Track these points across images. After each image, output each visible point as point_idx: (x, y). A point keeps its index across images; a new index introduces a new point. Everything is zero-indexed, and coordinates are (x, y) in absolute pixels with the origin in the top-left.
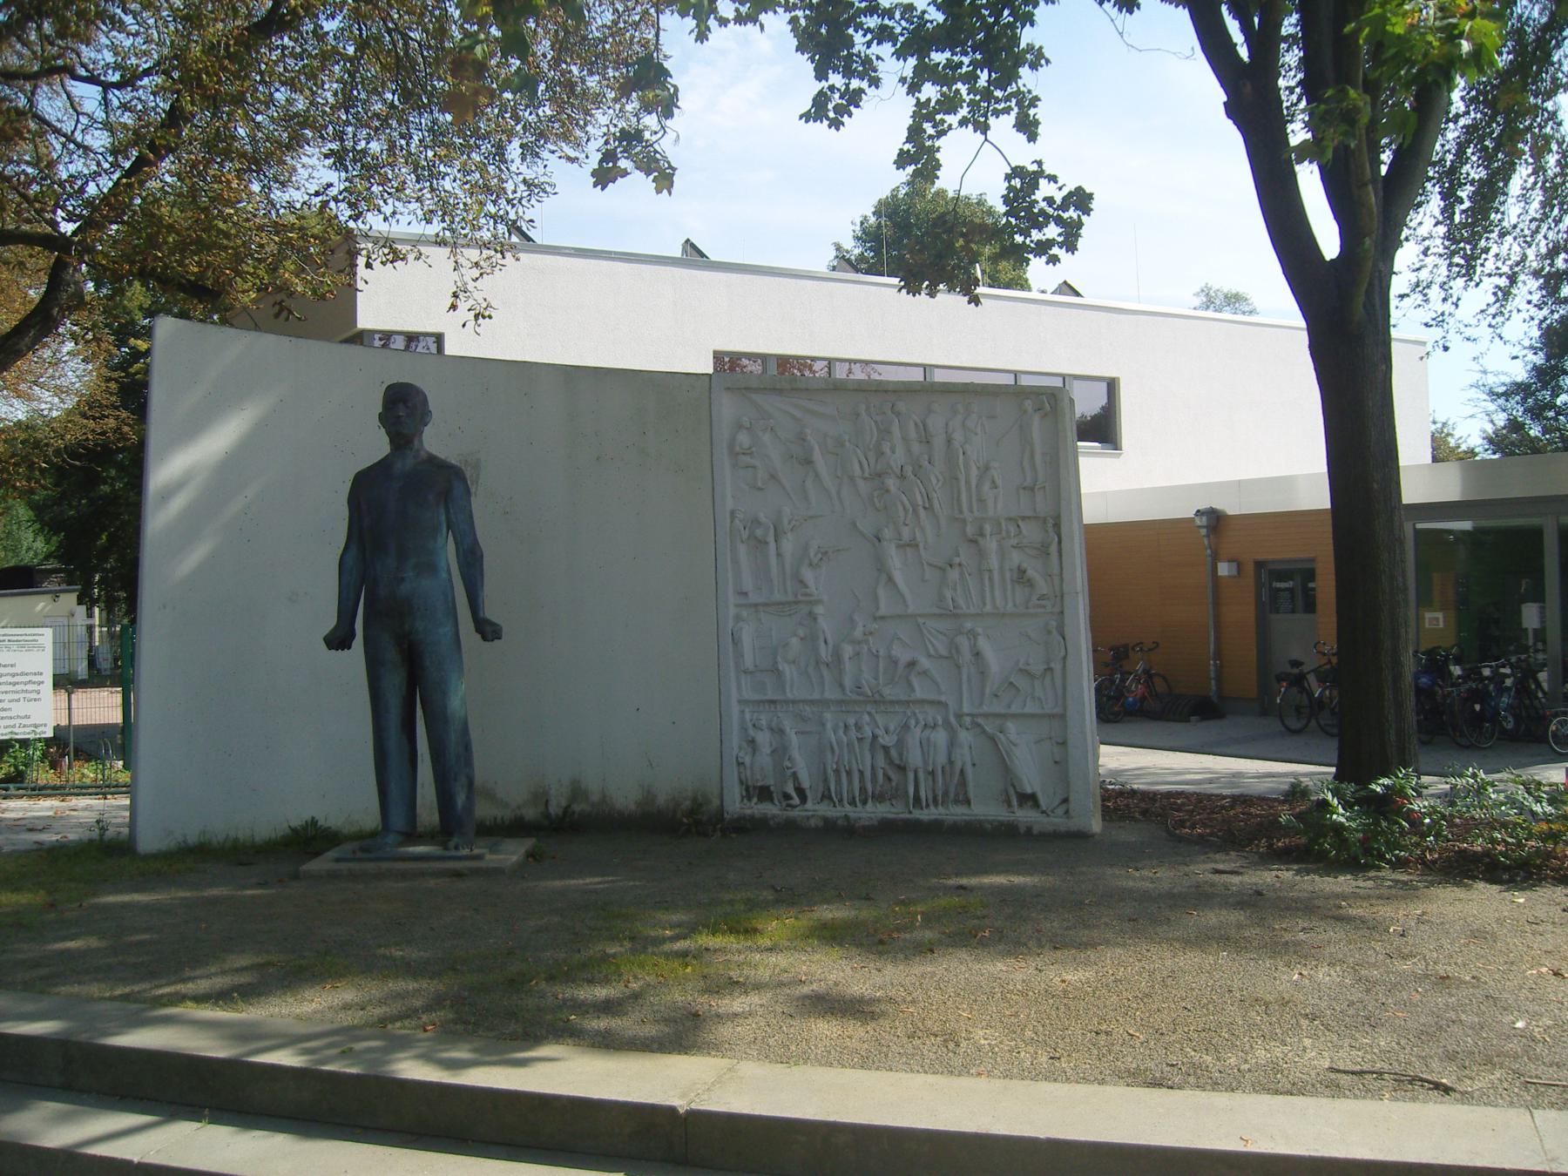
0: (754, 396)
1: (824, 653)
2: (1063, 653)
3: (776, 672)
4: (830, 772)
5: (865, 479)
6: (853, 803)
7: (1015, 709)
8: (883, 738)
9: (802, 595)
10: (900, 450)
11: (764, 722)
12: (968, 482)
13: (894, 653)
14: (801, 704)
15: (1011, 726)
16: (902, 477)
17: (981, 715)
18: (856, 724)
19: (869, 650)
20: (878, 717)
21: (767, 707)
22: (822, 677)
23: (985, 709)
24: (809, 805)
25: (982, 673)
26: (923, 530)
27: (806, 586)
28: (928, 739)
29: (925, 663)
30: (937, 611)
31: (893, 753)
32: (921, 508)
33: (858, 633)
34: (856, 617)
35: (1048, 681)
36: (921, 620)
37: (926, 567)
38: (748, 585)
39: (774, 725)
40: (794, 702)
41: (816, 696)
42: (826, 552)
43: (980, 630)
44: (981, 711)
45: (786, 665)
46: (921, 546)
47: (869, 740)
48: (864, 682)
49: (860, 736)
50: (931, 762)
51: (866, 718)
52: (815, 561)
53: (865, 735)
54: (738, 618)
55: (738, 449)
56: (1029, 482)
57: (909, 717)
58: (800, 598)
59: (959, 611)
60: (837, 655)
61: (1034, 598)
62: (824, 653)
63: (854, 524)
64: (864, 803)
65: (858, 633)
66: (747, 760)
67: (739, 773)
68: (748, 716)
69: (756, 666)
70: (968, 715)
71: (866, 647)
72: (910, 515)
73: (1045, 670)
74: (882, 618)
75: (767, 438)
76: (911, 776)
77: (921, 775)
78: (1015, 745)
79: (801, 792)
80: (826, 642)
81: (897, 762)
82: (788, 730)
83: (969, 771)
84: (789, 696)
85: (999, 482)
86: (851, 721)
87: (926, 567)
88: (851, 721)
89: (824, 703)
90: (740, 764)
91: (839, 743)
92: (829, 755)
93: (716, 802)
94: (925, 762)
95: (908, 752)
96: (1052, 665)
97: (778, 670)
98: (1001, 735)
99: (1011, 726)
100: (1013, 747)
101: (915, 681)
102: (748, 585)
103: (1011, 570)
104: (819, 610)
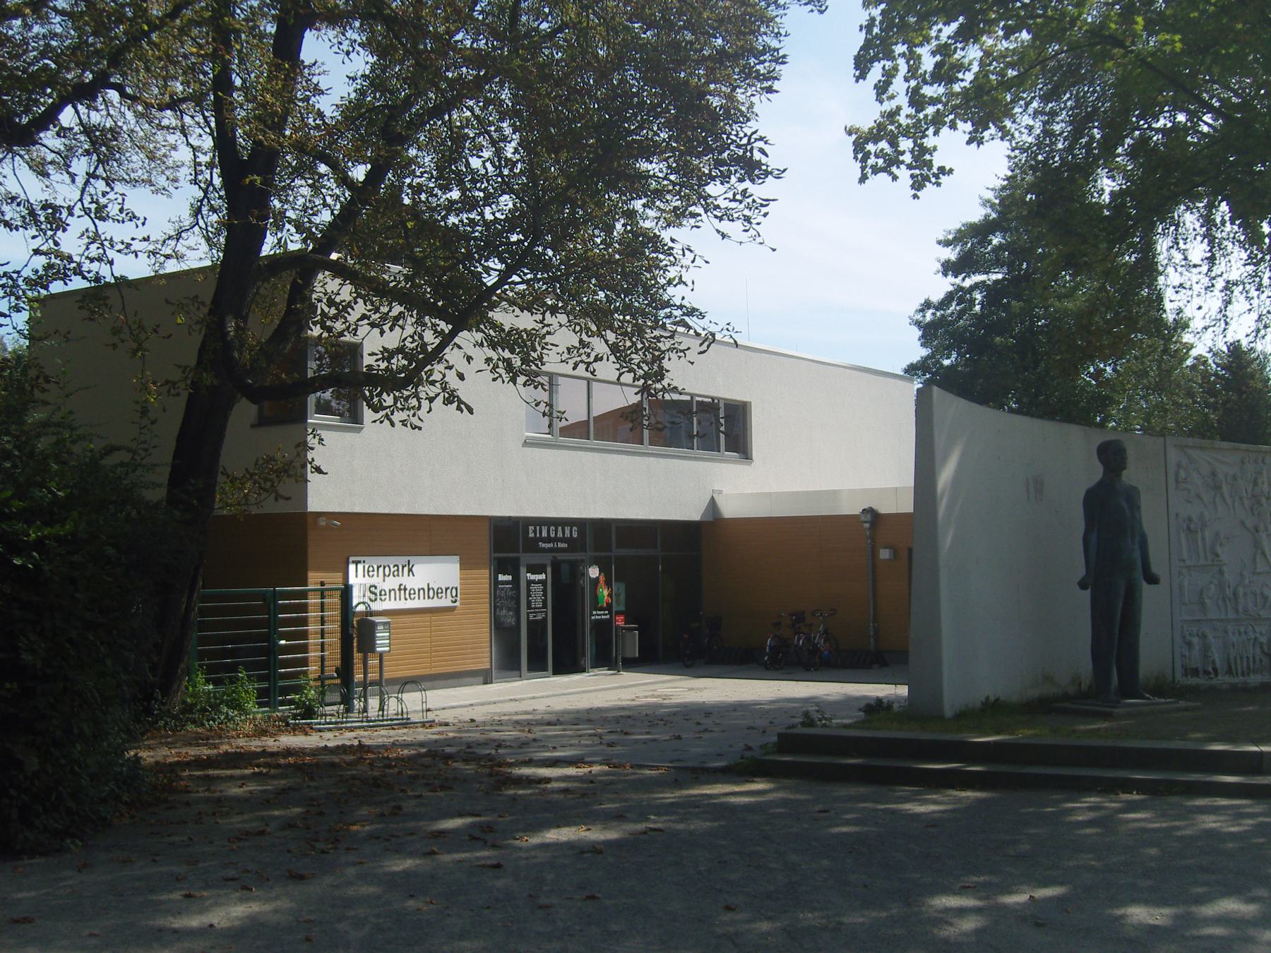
0: (1190, 451)
1: (1228, 592)
3: (1202, 603)
4: (1232, 657)
6: (1243, 675)
22: (1227, 606)
24: (1219, 677)
27: (1217, 556)
38: (1185, 555)
40: (1211, 620)
54: (1180, 573)
60: (1235, 594)
62: (1228, 592)
64: (1249, 674)
65: (1247, 581)
74: (1259, 573)
79: (1215, 670)
86: (1242, 630)
88: (1242, 630)
90: (1183, 656)
93: (1170, 679)
102: (1185, 555)
104: (1225, 569)
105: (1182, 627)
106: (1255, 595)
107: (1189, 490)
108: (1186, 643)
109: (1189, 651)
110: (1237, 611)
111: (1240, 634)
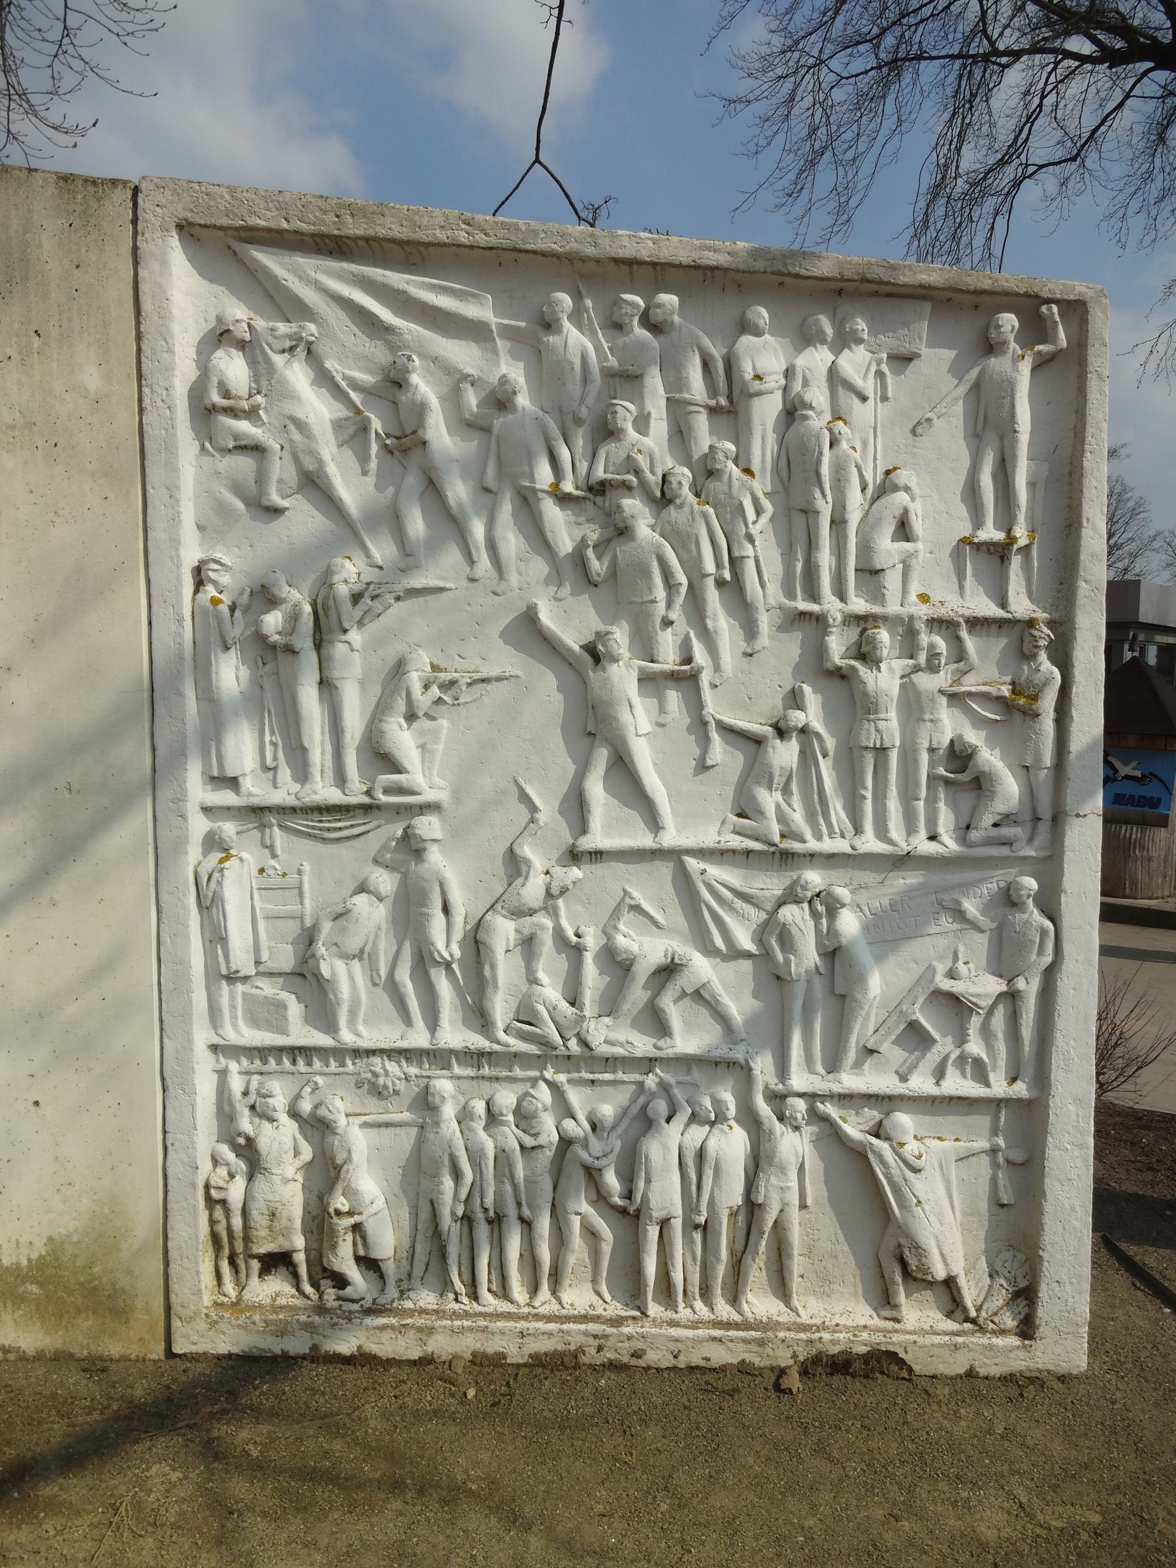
2: (1048, 959)
4: (446, 1221)
5: (563, 499)
7: (921, 1083)
8: (585, 1144)
9: (387, 791)
10: (660, 426)
11: (279, 1104)
12: (838, 522)
13: (621, 941)
14: (376, 1060)
15: (904, 1121)
16: (663, 499)
17: (831, 1097)
18: (518, 1111)
19: (559, 933)
20: (574, 1096)
21: (287, 1063)
23: (849, 1081)
25: (843, 997)
26: (708, 638)
27: (397, 768)
28: (701, 1154)
29: (701, 967)
30: (736, 842)
31: (612, 1180)
32: (710, 582)
33: (532, 890)
34: (527, 851)
35: (999, 1021)
36: (692, 863)
37: (715, 736)
39: (306, 1107)
40: (357, 1053)
41: (419, 1038)
42: (453, 683)
43: (843, 893)
44: (837, 1088)
45: (340, 965)
46: (705, 678)
47: (549, 1153)
48: (541, 1009)
49: (529, 1141)
50: (704, 1207)
51: (544, 1094)
52: (423, 700)
53: (542, 1140)
54: (213, 842)
55: (216, 398)
56: (991, 533)
57: (652, 1095)
58: (383, 798)
59: (796, 846)
61: (987, 820)
63: (530, 617)
65: (532, 890)
66: (236, 1192)
67: (212, 1222)
68: (236, 1084)
69: (258, 963)
70: (800, 1095)
71: (549, 923)
72: (680, 600)
73: (1001, 996)
74: (597, 855)
75: (297, 375)
76: (653, 1232)
77: (677, 1224)
78: (916, 1171)
79: (369, 1263)
80: (446, 909)
81: (617, 1201)
82: (342, 1121)
83: (795, 1217)
84: (347, 1037)
85: (918, 525)
86: (506, 1098)
87: (715, 736)
88: (506, 1098)
89: (439, 1057)
91: (476, 1158)
92: (448, 1183)
94: (690, 1207)
95: (648, 1181)
96: (1021, 984)
97: (318, 976)
98: (883, 1146)
99: (904, 1121)
100: (909, 1174)
101: (674, 1013)
103: (932, 750)
104: (428, 826)
105: (223, 1074)
106: (575, 951)
107: (256, 449)
108: (235, 1148)
109: (250, 1178)
110: (480, 1018)
111: (493, 1118)
